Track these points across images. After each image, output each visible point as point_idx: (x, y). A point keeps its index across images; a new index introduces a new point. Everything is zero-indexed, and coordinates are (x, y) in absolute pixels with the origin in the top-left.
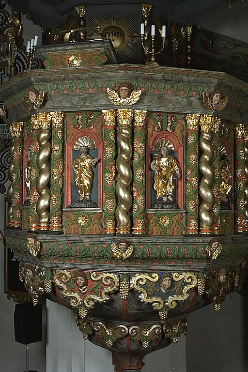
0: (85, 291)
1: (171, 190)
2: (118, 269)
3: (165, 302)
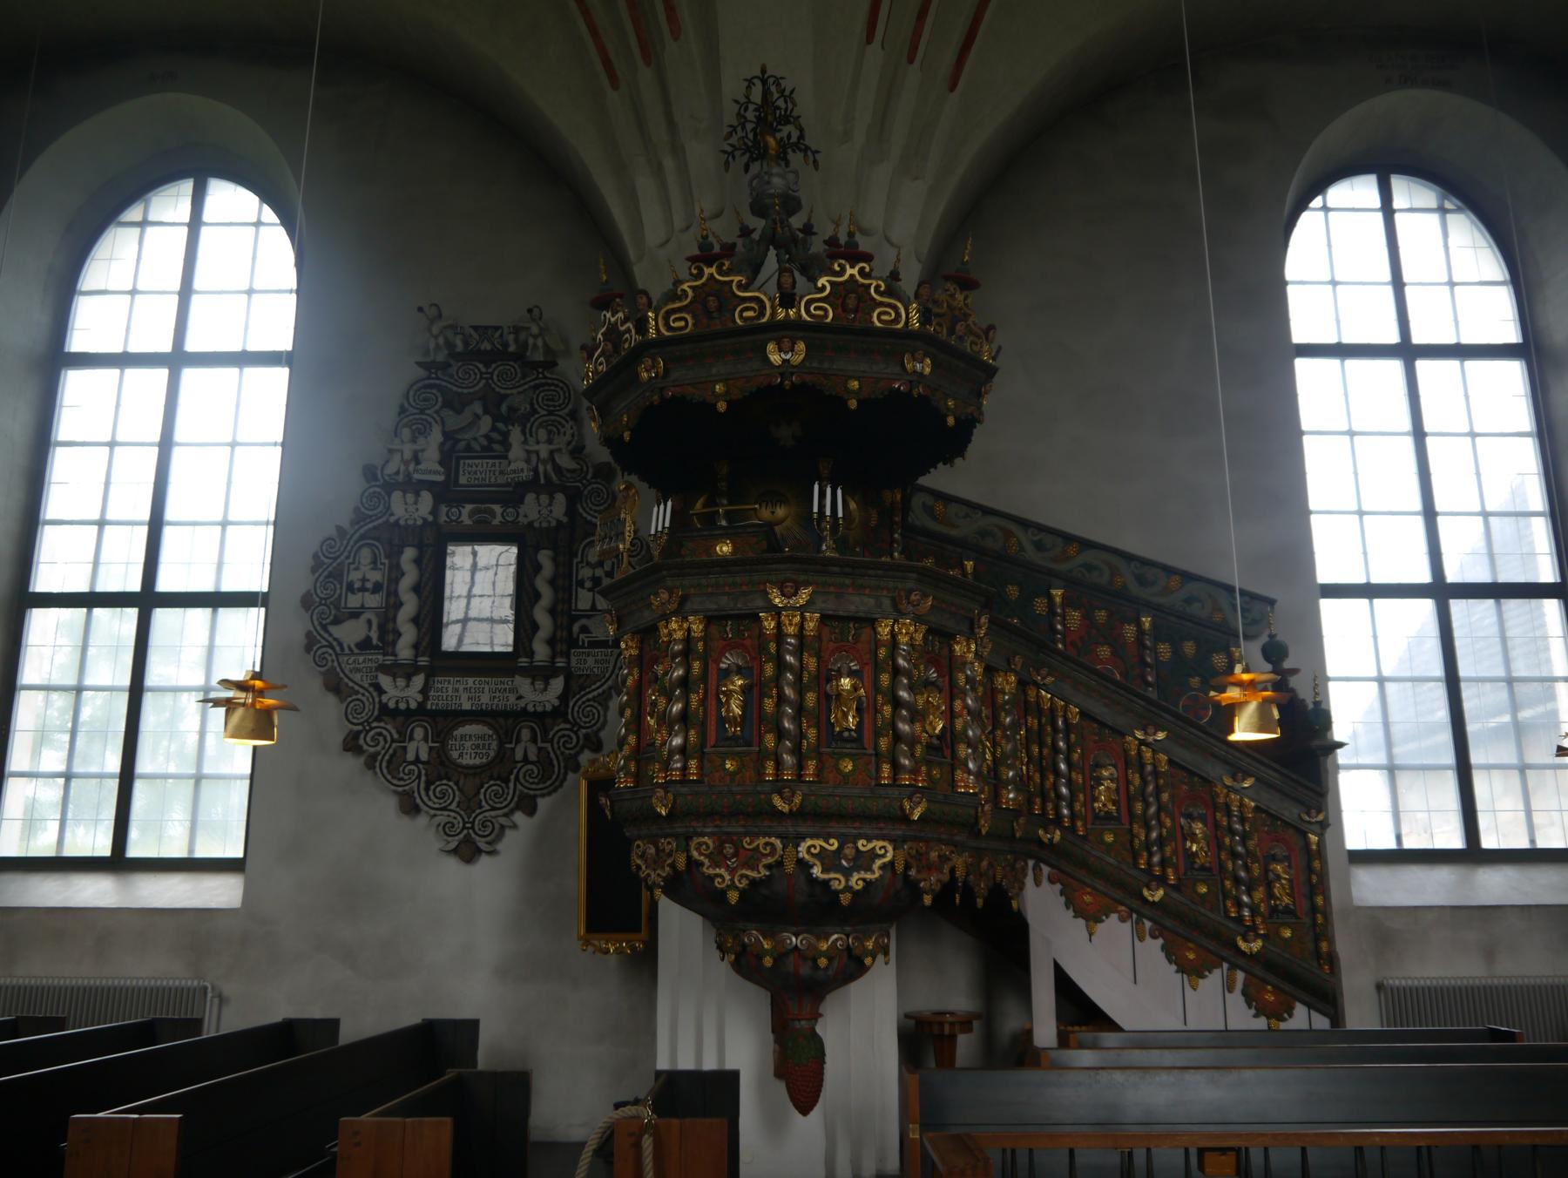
0: (735, 865)
1: (855, 723)
2: (781, 829)
3: (847, 881)
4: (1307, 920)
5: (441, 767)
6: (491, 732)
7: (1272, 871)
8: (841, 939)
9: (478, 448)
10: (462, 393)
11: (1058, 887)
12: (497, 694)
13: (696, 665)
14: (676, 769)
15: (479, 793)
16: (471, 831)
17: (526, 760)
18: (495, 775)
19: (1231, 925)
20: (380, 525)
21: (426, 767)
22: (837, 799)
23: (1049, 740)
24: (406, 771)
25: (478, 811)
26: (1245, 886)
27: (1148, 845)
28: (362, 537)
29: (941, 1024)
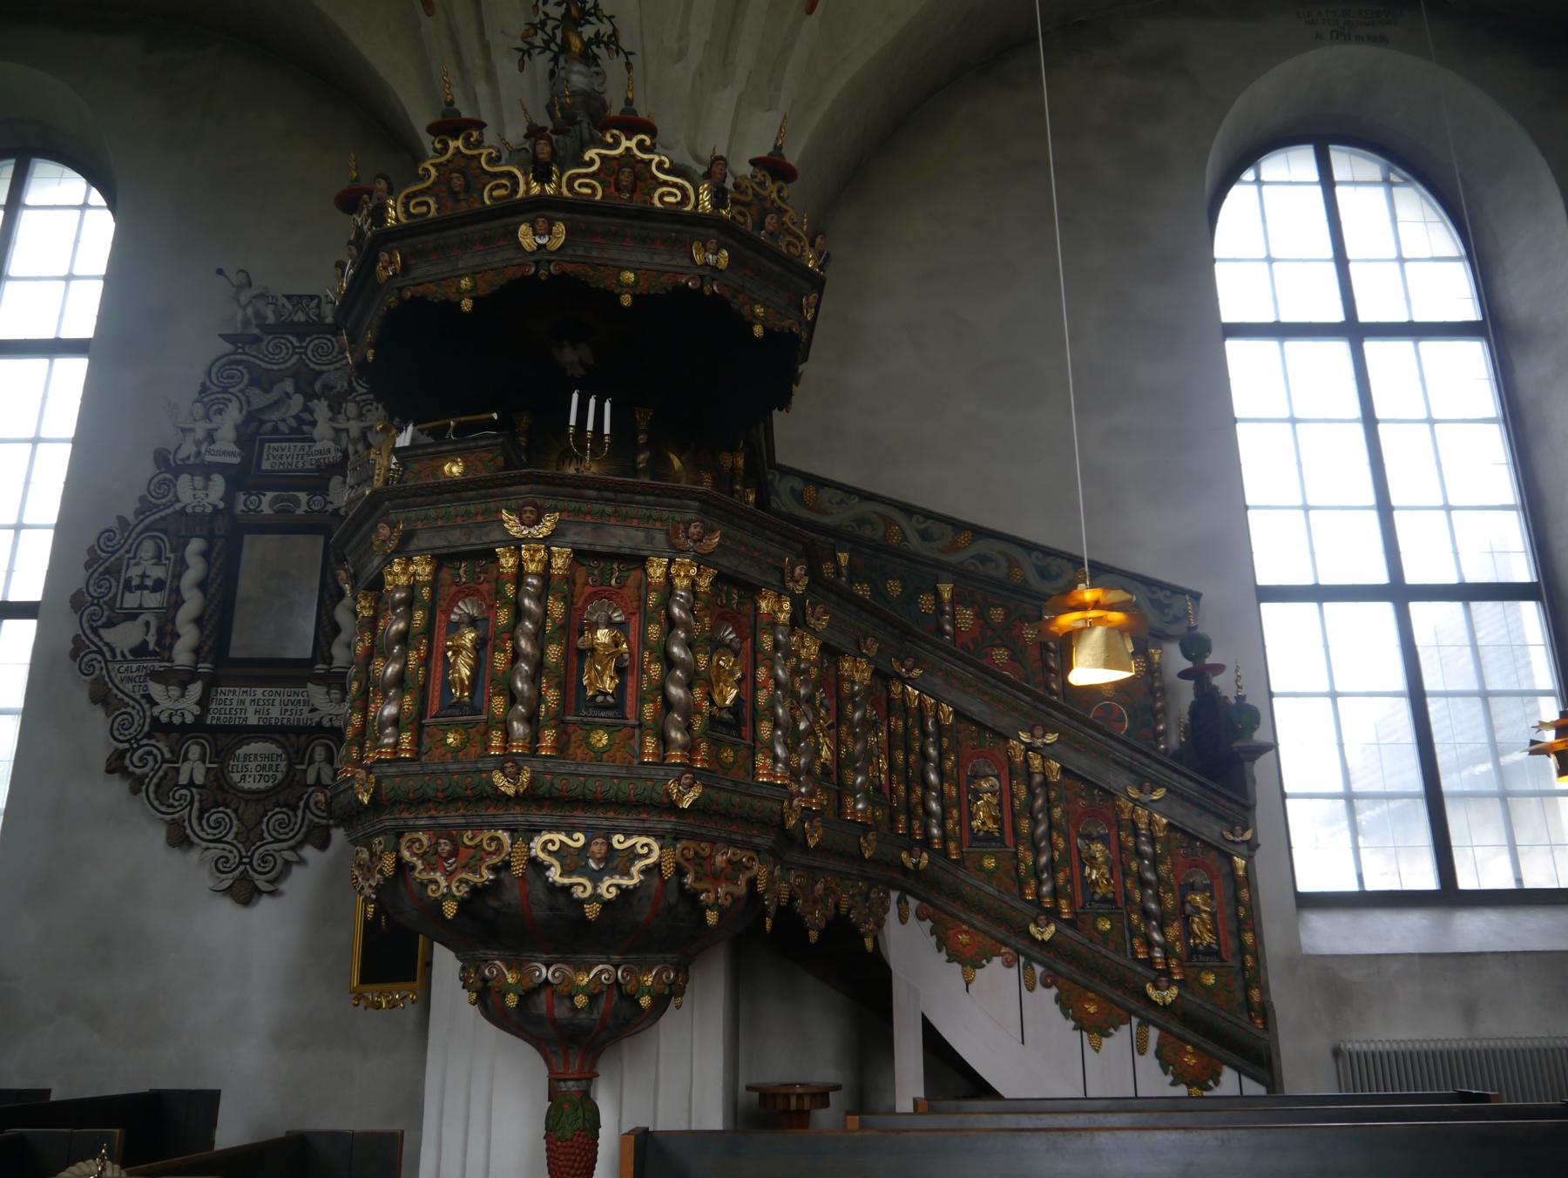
1: (613, 685)
3: (595, 887)
4: (1234, 963)
5: (218, 792)
6: (280, 751)
7: (1190, 902)
8: (607, 971)
9: (286, 430)
10: (272, 370)
11: (928, 924)
12: (290, 707)
13: (419, 615)
14: (387, 745)
15: (261, 822)
16: (248, 867)
17: (318, 781)
18: (282, 800)
19: (1139, 969)
20: (168, 515)
21: (200, 791)
22: (582, 779)
23: (917, 746)
24: (177, 796)
25: (258, 844)
26: (1156, 920)
27: (1036, 872)
28: (147, 529)
29: (787, 1097)
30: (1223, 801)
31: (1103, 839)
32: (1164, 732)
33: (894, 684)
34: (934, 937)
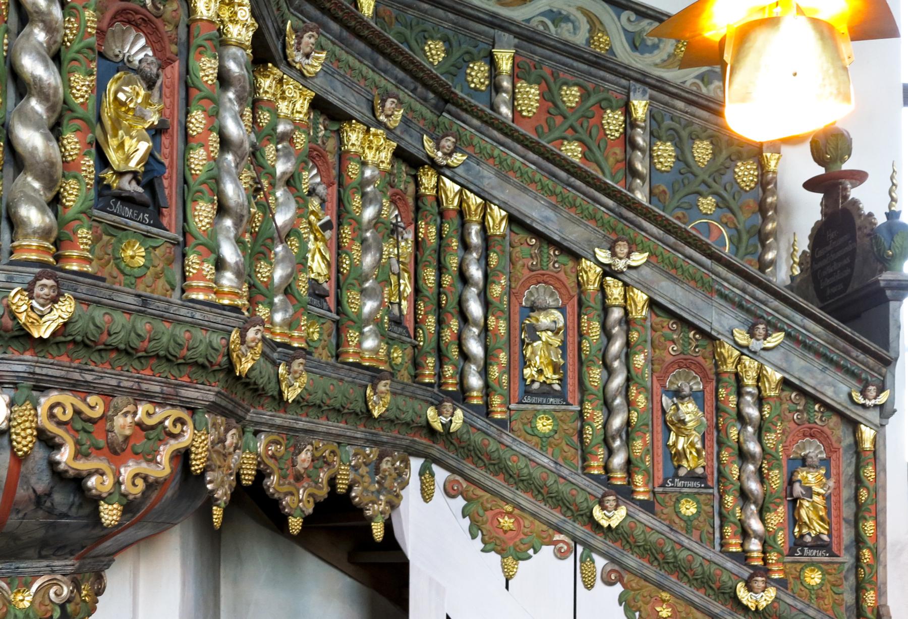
4: (847, 559)
7: (800, 481)
11: (460, 502)
19: (729, 565)
26: (755, 503)
30: (855, 353)
31: (698, 398)
32: (772, 263)
33: (425, 174)
34: (467, 518)
